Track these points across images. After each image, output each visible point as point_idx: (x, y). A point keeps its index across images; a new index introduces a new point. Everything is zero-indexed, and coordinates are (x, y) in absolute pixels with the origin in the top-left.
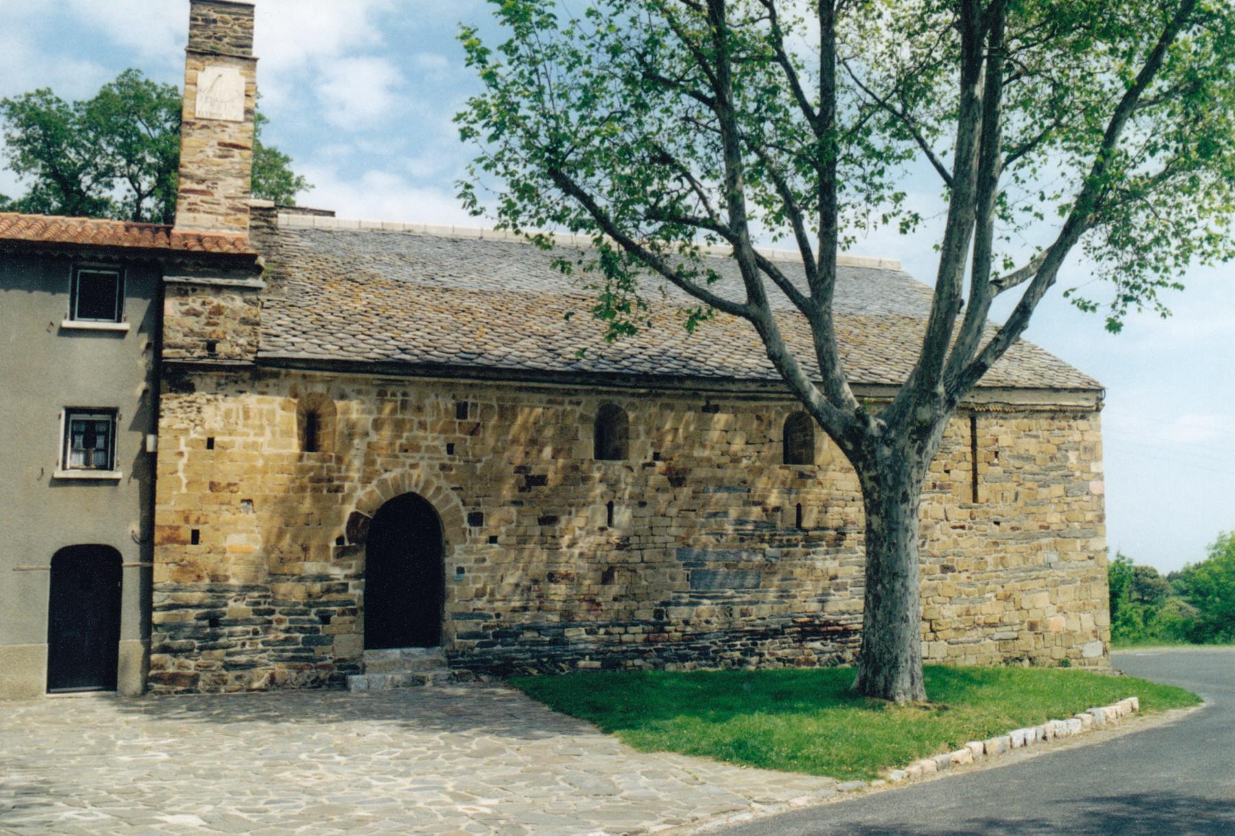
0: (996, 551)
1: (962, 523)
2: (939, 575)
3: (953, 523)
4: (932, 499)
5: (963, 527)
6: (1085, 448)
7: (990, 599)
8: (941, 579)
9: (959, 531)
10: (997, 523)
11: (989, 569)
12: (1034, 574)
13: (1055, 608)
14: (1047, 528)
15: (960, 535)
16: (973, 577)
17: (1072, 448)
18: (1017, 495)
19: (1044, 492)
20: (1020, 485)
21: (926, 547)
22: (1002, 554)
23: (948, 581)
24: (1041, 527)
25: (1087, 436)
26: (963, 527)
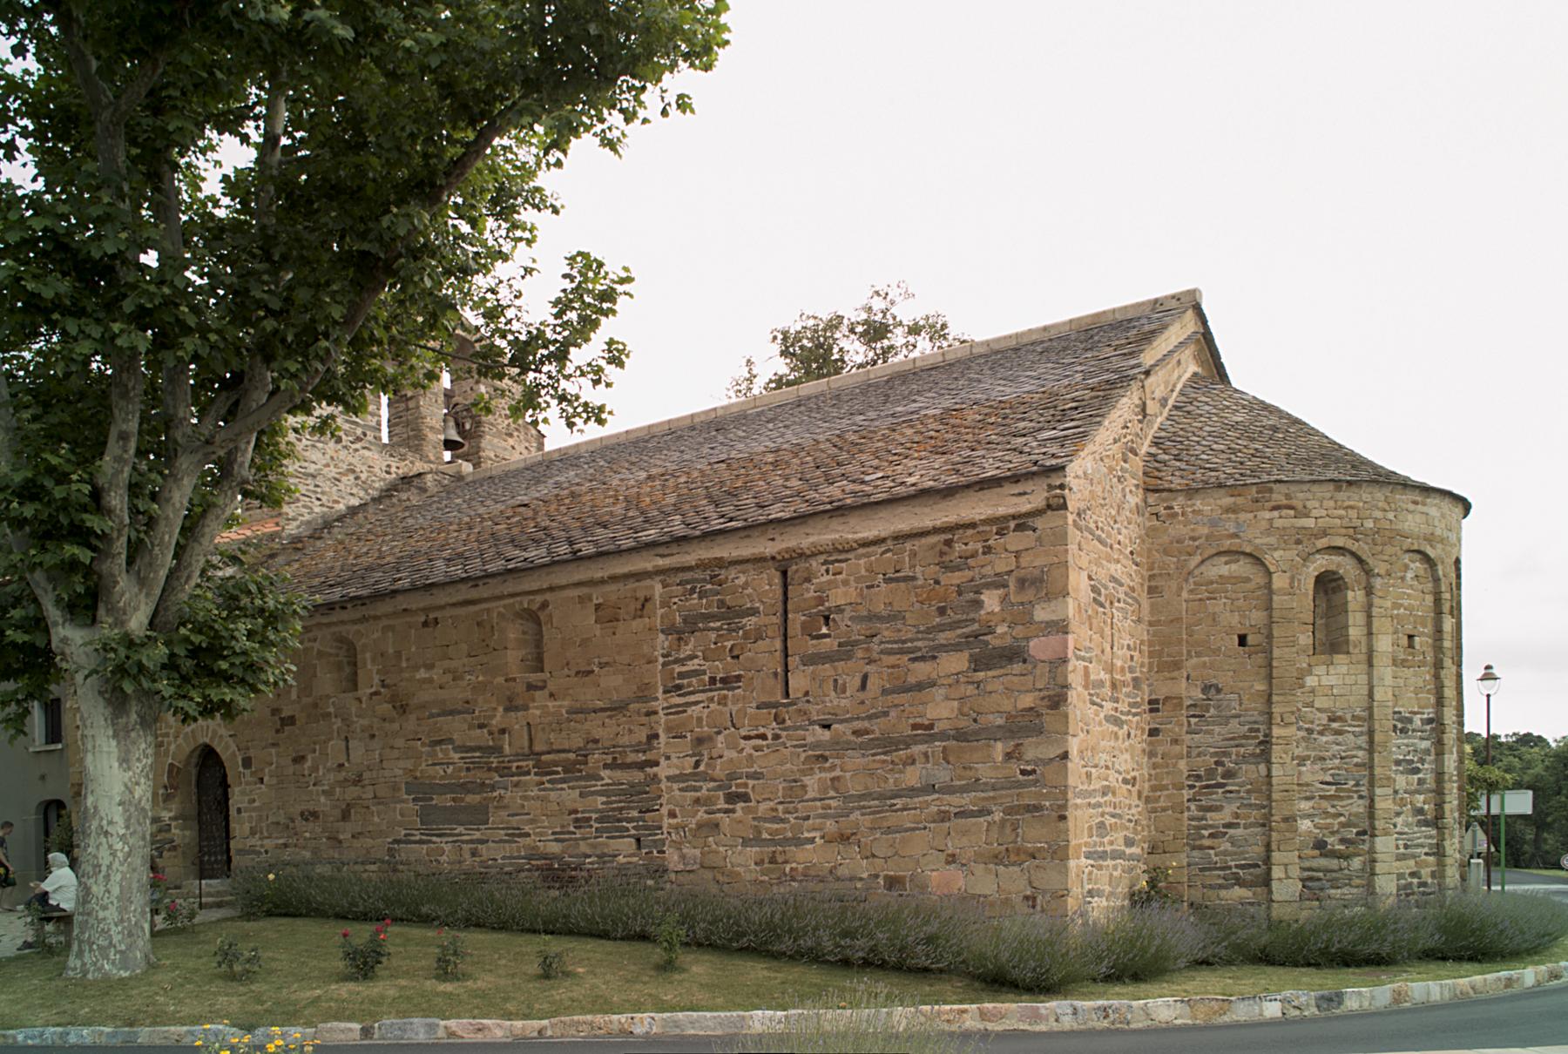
0: (822, 770)
1: (762, 730)
2: (722, 805)
3: (743, 732)
4: (711, 700)
5: (763, 737)
6: (1022, 583)
7: (812, 840)
8: (726, 811)
9: (760, 742)
10: (828, 727)
11: (810, 795)
12: (899, 802)
13: (942, 856)
14: (931, 726)
15: (757, 749)
16: (780, 807)
17: (988, 586)
18: (865, 678)
19: (922, 670)
20: (870, 662)
21: (702, 768)
22: (837, 773)
23: (739, 813)
24: (915, 727)
25: (1025, 560)
26: (763, 737)
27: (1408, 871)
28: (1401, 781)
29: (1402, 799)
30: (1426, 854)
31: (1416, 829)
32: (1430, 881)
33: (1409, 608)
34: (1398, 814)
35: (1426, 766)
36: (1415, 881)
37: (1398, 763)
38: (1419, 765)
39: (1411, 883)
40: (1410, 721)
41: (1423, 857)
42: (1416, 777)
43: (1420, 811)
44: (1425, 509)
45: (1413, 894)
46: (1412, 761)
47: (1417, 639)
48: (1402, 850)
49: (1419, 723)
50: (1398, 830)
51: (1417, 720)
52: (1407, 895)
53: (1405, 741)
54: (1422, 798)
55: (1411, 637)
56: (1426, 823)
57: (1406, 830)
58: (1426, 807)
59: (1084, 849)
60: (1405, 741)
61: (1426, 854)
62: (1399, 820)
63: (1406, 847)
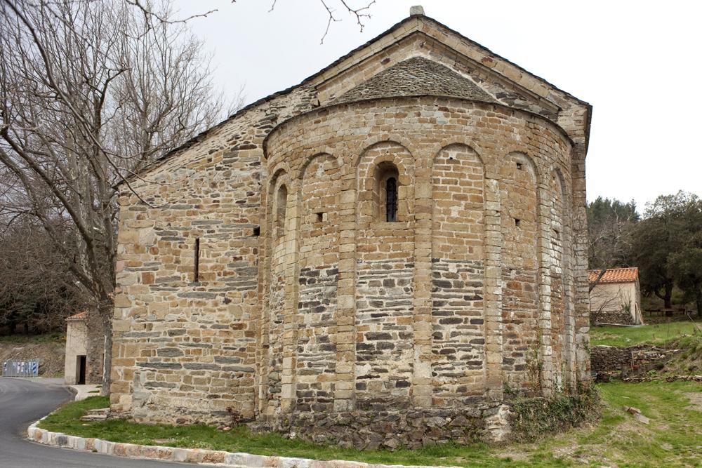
27: (310, 383)
28: (309, 318)
29: (308, 330)
30: (326, 371)
31: (319, 352)
32: (328, 391)
33: (320, 195)
34: (306, 342)
35: (331, 305)
36: (316, 391)
37: (306, 305)
38: (325, 306)
39: (311, 392)
40: (317, 274)
41: (324, 373)
42: (321, 314)
43: (324, 339)
44: (326, 123)
45: (313, 400)
46: (319, 303)
47: (325, 215)
48: (306, 367)
49: (326, 274)
50: (303, 353)
51: (323, 273)
52: (307, 401)
53: (312, 289)
54: (326, 329)
55: (320, 215)
56: (329, 348)
57: (311, 353)
58: (330, 336)
59: (136, 361)
60: (312, 289)
61: (326, 371)
62: (305, 346)
63: (310, 365)
